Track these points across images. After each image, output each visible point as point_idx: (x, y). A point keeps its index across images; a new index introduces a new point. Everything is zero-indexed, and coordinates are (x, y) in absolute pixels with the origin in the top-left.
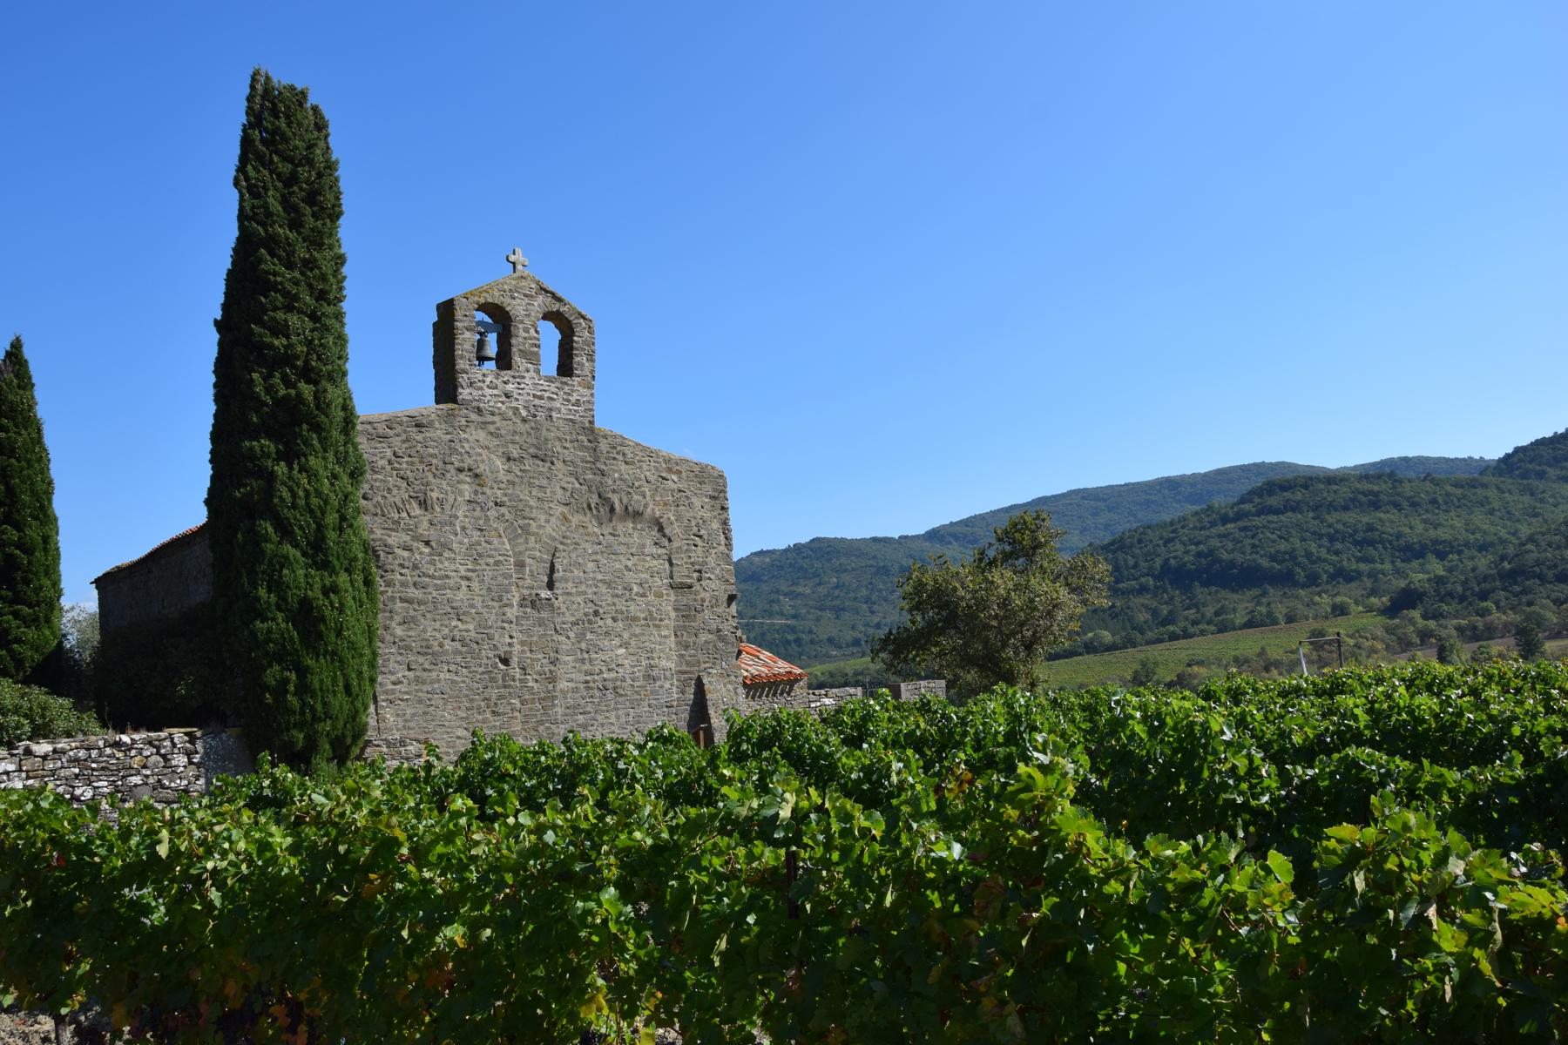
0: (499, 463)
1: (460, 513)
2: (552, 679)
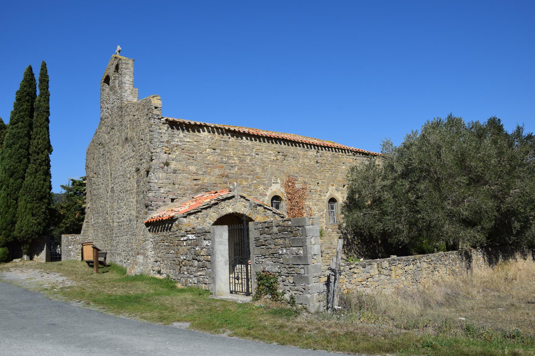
0: (107, 137)
1: (101, 161)
2: (113, 222)
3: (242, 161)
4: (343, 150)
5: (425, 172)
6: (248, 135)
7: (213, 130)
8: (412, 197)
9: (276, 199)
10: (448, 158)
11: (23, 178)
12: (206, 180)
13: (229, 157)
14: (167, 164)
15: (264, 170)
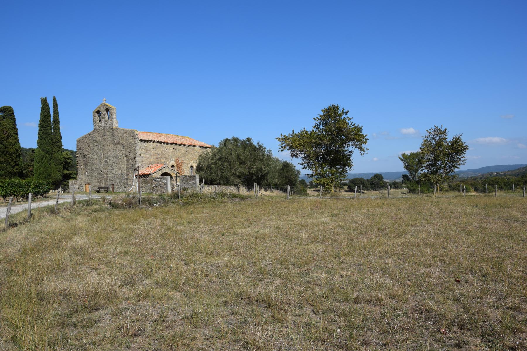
3: (162, 152)
4: (196, 146)
5: (226, 159)
6: (164, 143)
7: (153, 142)
8: (222, 167)
9: (173, 166)
10: (234, 156)
11: (52, 154)
12: (152, 160)
13: (158, 151)
14: (140, 155)
15: (169, 156)
